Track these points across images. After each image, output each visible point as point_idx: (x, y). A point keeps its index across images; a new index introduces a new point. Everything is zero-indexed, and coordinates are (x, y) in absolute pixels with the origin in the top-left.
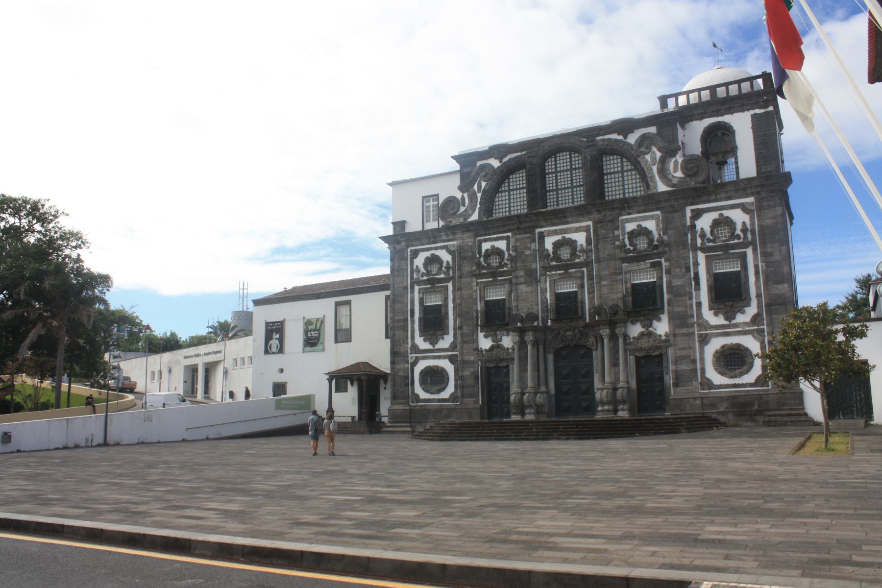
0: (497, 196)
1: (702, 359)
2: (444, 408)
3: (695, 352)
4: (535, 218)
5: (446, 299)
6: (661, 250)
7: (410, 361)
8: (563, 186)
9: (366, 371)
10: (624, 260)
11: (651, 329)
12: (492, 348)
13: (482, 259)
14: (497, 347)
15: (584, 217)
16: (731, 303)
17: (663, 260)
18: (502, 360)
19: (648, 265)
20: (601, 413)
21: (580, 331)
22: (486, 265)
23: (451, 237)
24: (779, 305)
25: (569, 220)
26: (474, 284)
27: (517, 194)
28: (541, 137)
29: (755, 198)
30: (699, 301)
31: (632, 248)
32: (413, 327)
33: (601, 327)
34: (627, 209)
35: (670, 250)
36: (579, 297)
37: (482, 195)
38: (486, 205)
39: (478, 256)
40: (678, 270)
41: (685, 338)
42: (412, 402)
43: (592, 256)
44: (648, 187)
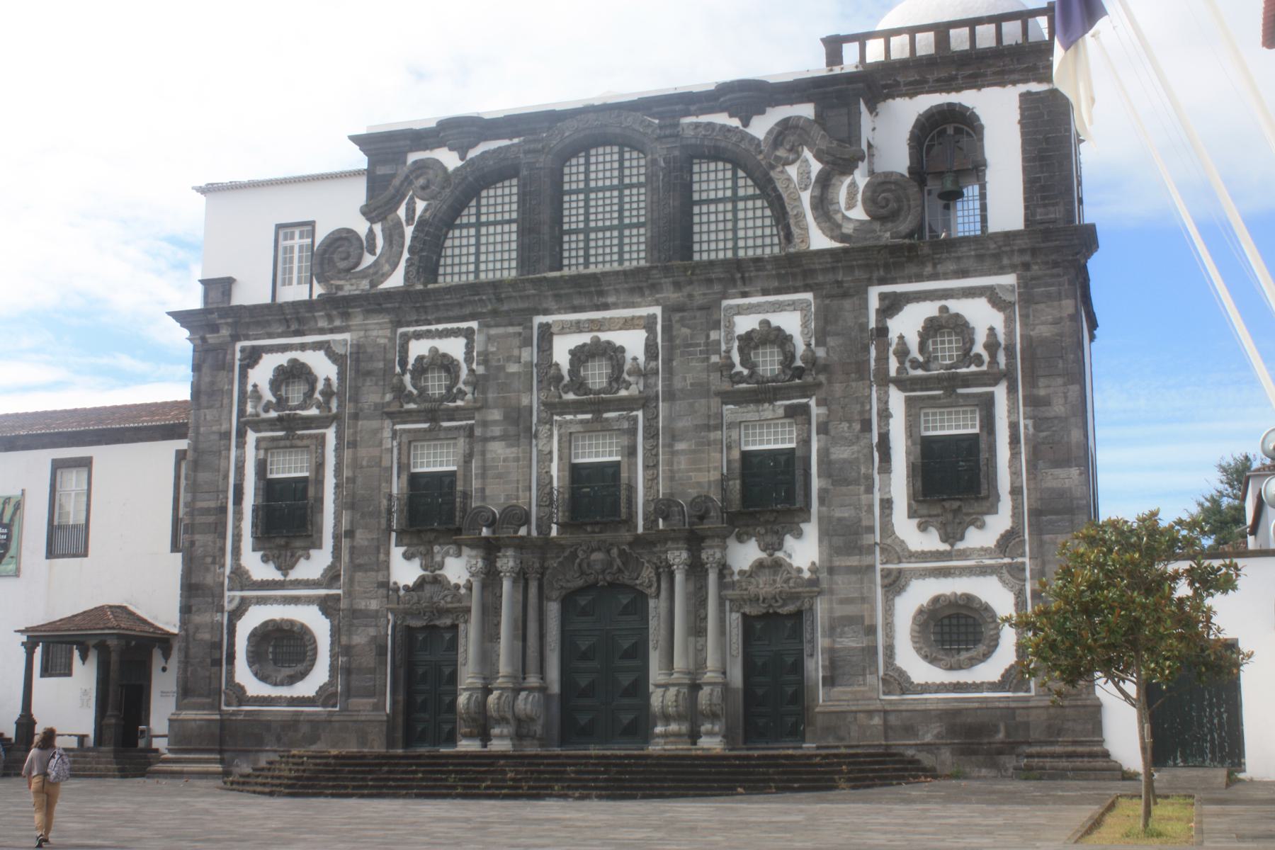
0: (450, 235)
1: (889, 626)
2: (302, 718)
3: (873, 609)
4: (533, 292)
5: (320, 466)
6: (809, 379)
7: (228, 607)
8: (600, 224)
9: (120, 628)
10: (728, 397)
11: (779, 554)
12: (421, 584)
13: (407, 378)
14: (432, 581)
15: (643, 295)
16: (956, 504)
17: (813, 402)
18: (443, 612)
19: (781, 412)
20: (662, 741)
21: (622, 553)
22: (415, 392)
23: (337, 323)
24: (1056, 512)
25: (611, 299)
26: (387, 434)
27: (495, 234)
28: (558, 108)
29: (1019, 278)
30: (886, 497)
31: (746, 372)
32: (237, 528)
33: (669, 544)
34: (739, 283)
35: (830, 382)
36: (624, 475)
37: (416, 230)
38: (424, 254)
39: (398, 369)
40: (845, 425)
41: (854, 578)
42: (228, 704)
43: (656, 385)
44: (789, 237)
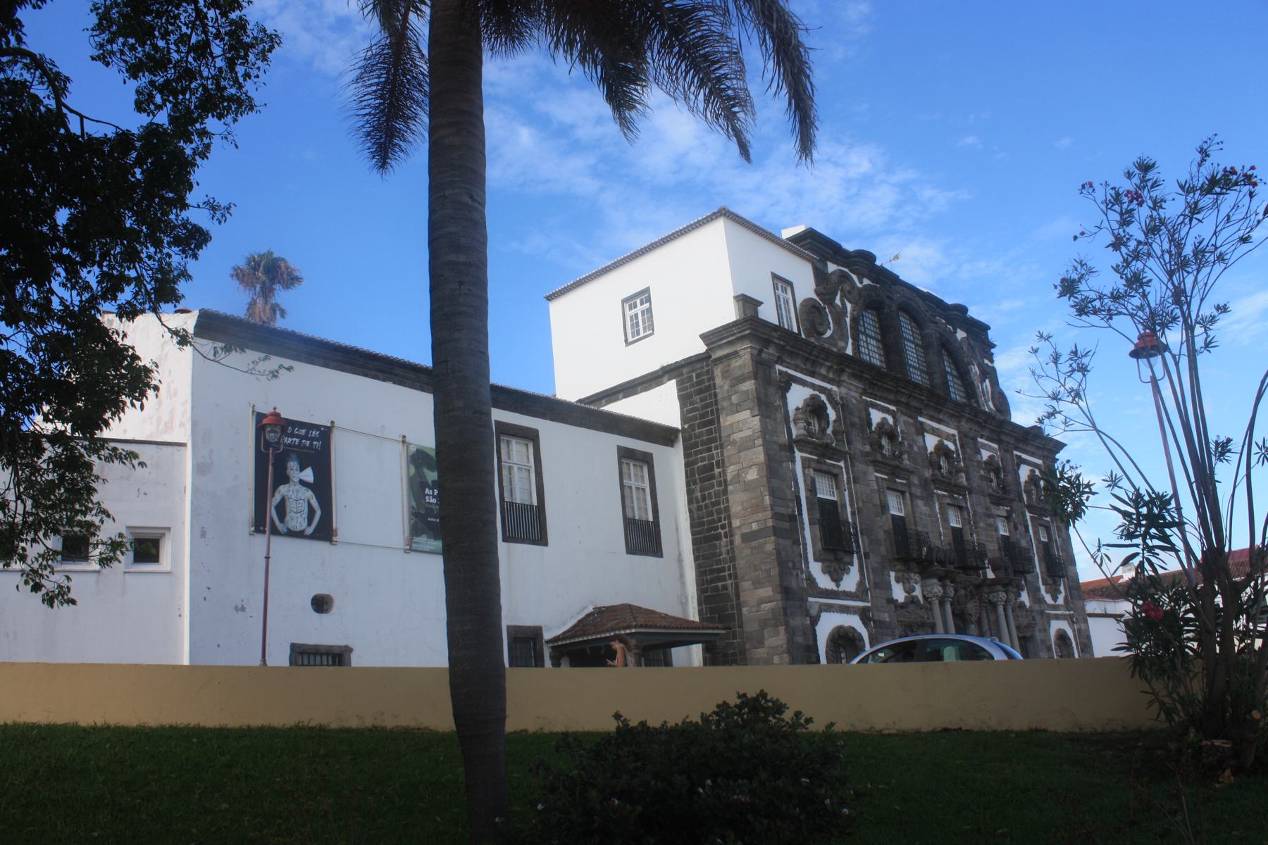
14: (912, 601)
23: (831, 375)
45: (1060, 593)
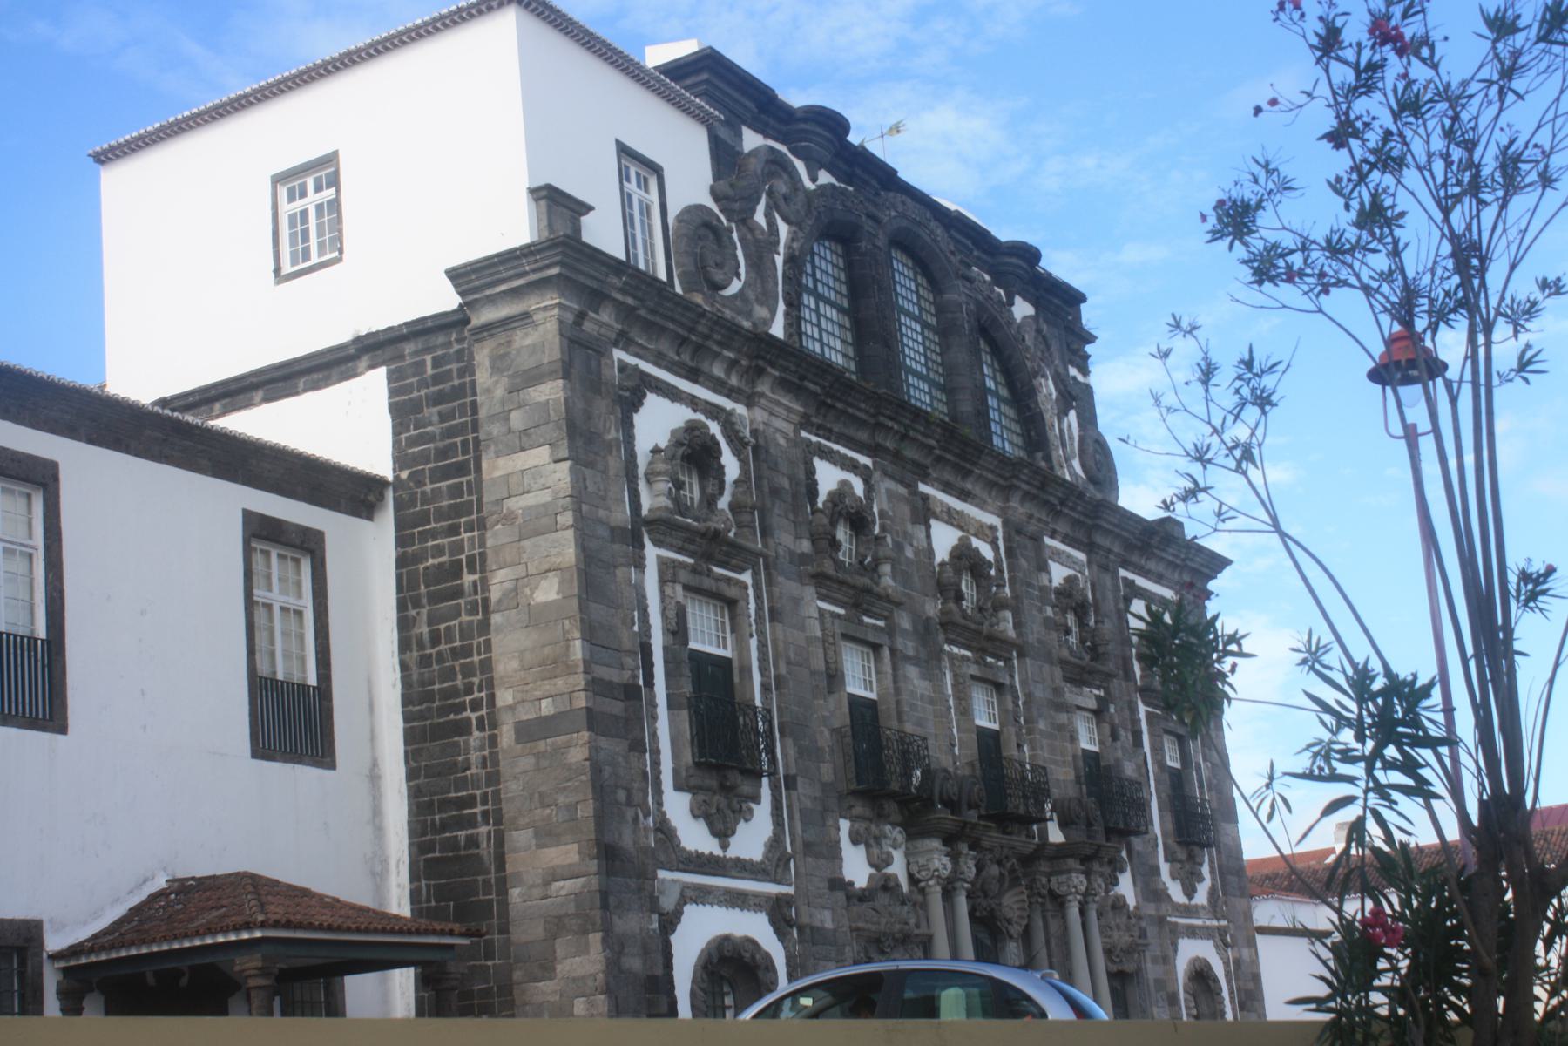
14: (884, 885)
23: (734, 381)
45: (1202, 879)
